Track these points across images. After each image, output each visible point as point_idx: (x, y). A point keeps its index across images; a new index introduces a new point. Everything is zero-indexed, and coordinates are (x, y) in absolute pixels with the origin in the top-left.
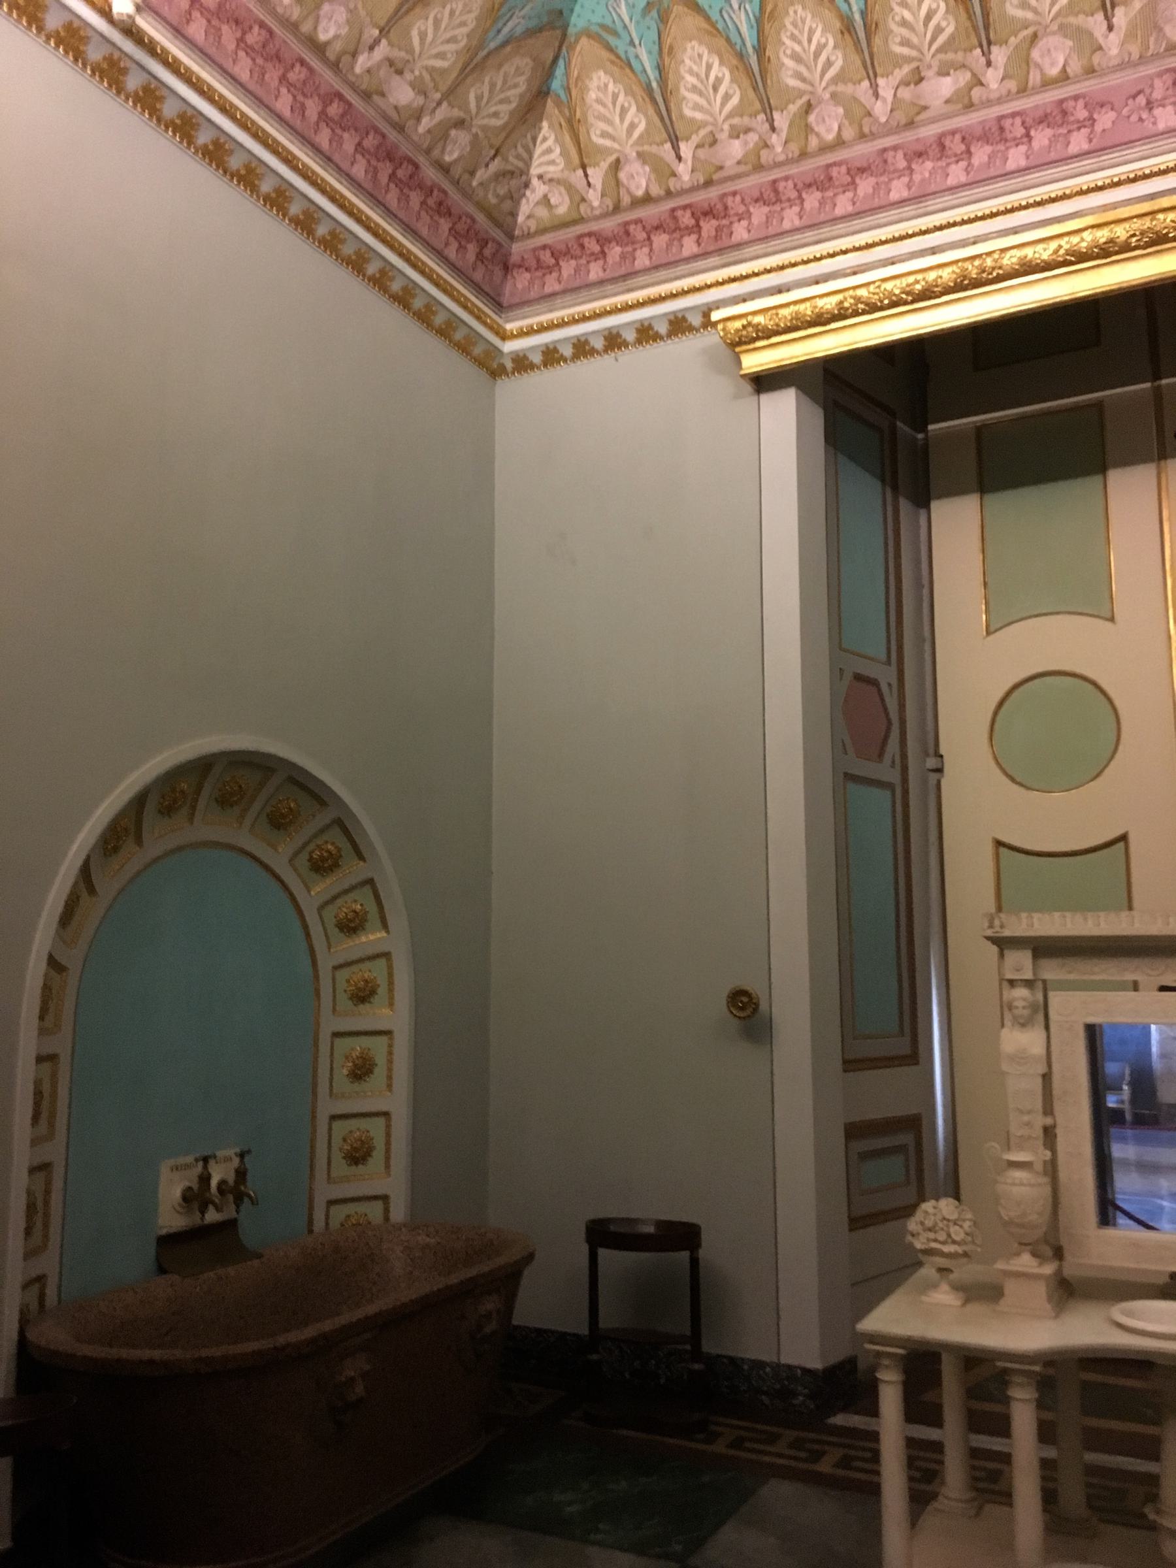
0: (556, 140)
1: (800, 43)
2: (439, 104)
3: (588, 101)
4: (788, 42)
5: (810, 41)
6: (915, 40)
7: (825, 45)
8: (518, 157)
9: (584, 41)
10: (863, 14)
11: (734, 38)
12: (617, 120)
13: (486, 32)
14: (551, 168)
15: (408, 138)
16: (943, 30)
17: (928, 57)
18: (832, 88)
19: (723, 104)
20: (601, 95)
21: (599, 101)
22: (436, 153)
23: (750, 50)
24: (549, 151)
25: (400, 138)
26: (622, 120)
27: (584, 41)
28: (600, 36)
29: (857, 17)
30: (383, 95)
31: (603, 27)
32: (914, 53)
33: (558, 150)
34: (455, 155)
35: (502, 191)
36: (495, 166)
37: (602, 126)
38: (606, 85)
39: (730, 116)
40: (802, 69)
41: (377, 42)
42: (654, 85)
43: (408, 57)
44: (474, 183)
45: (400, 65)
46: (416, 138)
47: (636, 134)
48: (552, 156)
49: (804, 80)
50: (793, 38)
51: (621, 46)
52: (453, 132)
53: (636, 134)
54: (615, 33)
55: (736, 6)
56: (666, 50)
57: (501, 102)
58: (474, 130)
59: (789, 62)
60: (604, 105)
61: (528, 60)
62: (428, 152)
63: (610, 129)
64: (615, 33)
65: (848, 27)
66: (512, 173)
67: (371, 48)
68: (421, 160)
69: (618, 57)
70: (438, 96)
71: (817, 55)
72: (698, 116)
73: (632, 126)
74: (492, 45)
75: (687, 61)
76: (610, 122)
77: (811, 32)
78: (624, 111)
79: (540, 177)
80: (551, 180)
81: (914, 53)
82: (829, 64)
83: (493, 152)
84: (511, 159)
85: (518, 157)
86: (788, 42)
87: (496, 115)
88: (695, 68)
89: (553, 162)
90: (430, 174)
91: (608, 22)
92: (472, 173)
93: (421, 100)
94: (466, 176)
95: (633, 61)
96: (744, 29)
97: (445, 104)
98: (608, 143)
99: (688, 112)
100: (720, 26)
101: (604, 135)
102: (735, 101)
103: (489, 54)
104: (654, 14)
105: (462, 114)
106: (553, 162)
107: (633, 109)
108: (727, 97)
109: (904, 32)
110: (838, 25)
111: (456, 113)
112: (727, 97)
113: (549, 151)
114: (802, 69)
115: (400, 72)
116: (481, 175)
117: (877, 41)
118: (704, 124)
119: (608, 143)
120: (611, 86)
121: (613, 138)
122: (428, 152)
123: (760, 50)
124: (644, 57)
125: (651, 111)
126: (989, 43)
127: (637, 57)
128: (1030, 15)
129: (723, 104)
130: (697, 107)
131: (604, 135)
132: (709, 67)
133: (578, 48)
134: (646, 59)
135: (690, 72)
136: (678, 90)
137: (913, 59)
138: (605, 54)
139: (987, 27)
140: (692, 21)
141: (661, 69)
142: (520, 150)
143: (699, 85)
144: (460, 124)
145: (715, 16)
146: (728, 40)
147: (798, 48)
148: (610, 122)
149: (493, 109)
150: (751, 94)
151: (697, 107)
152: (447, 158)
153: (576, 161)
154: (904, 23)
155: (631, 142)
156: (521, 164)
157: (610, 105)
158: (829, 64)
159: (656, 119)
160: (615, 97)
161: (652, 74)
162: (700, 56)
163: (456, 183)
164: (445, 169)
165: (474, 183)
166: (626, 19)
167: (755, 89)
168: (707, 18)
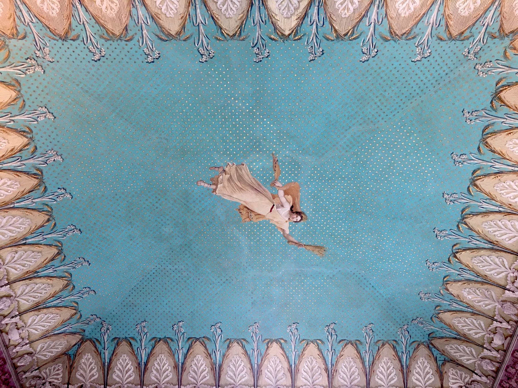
0: (62, 372)
1: (160, 366)
2: (26, 344)
3: (81, 362)
4: (156, 365)
5: (163, 367)
6: (196, 377)
7: (168, 370)
8: (46, 373)
9: (88, 342)
10: (183, 364)
11: (139, 358)
12: (88, 371)
13: (56, 327)
14: (56, 381)
15: (8, 352)
16: (206, 377)
17: (199, 384)
18: (166, 384)
19: (127, 379)
20: (86, 361)
21: (84, 363)
22: (15, 361)
23: (143, 363)
24: (58, 374)
25: (5, 351)
26: (90, 372)
27: (88, 342)
28: (94, 342)
29: (180, 364)
30: (7, 334)
31: (97, 340)
32: (195, 382)
33: (61, 375)
34: (22, 364)
35: (33, 383)
36: (34, 373)
37: (82, 371)
38: (89, 359)
39: (128, 383)
40: (158, 375)
41: (16, 316)
42: (106, 364)
43: (25, 326)
44: (24, 377)
45: (19, 326)
46: (11, 353)
47: (92, 379)
48: (58, 377)
49: (157, 379)
50: (158, 364)
51: (100, 348)
52: (26, 356)
53: (92, 379)
54: (100, 343)
55: (143, 348)
56: (115, 354)
57: (49, 352)
58: (34, 358)
59: (155, 372)
60: (86, 365)
61: (66, 342)
62: (12, 359)
63: (84, 374)
64: (100, 343)
65: (176, 367)
66: (40, 377)
67: (13, 317)
68: (8, 361)
69: (98, 351)
70: (28, 341)
71: (164, 372)
72: (118, 379)
73: (93, 375)
74: (56, 332)
75: (121, 360)
76: (85, 372)
77: (165, 364)
78: (92, 369)
79: (50, 382)
80: (54, 385)
81: (195, 382)
82: (167, 376)
83: (37, 368)
84: (42, 373)
85: (46, 373)
86: (156, 365)
87: (45, 356)
88: (122, 363)
89: (58, 379)
90: (9, 367)
91: (99, 339)
92: (25, 372)
93: (20, 341)
94: (22, 373)
95: (102, 354)
96: (143, 356)
97: (28, 345)
98: (81, 378)
99: (114, 377)
100: (136, 352)
101: (81, 375)
102: (132, 378)
103: (54, 334)
104: (116, 341)
105: (32, 351)
106: (58, 379)
107: (96, 370)
108: (130, 376)
109: (194, 374)
110: (173, 365)
111: (31, 350)
112: (130, 376)
113: (58, 374)
114: (158, 375)
115: (18, 329)
116: (28, 374)
117: (185, 374)
118: (119, 383)
119: (81, 378)
120: (91, 360)
121: (84, 377)
122: (12, 359)
123: (146, 364)
124: (107, 354)
125: (101, 373)
126: (219, 386)
127: (104, 353)
128: (232, 381)
129: (127, 379)
130: (118, 376)
131: (81, 375)
132: (127, 364)
133: (85, 344)
134: (107, 355)
135: (120, 364)
136: (114, 368)
137: (194, 383)
138: (93, 349)
139: (219, 381)
140: (127, 348)
141: (110, 360)
142: (47, 371)
143: (122, 369)
144: (30, 354)
145: (135, 348)
146: (137, 358)
147: (159, 368)
148: (85, 372)
149: (45, 353)
150: (138, 378)
151: (118, 376)
152: (19, 364)
153: (66, 381)
154: (195, 372)
155: (90, 381)
156: (45, 376)
157: (88, 366)
158: (167, 376)
159: (102, 376)
160: (91, 363)
161: (107, 360)
162: (126, 360)
163: (17, 374)
164: (15, 367)
165: (24, 377)
166: (106, 340)
167: (140, 376)
168: (132, 349)
